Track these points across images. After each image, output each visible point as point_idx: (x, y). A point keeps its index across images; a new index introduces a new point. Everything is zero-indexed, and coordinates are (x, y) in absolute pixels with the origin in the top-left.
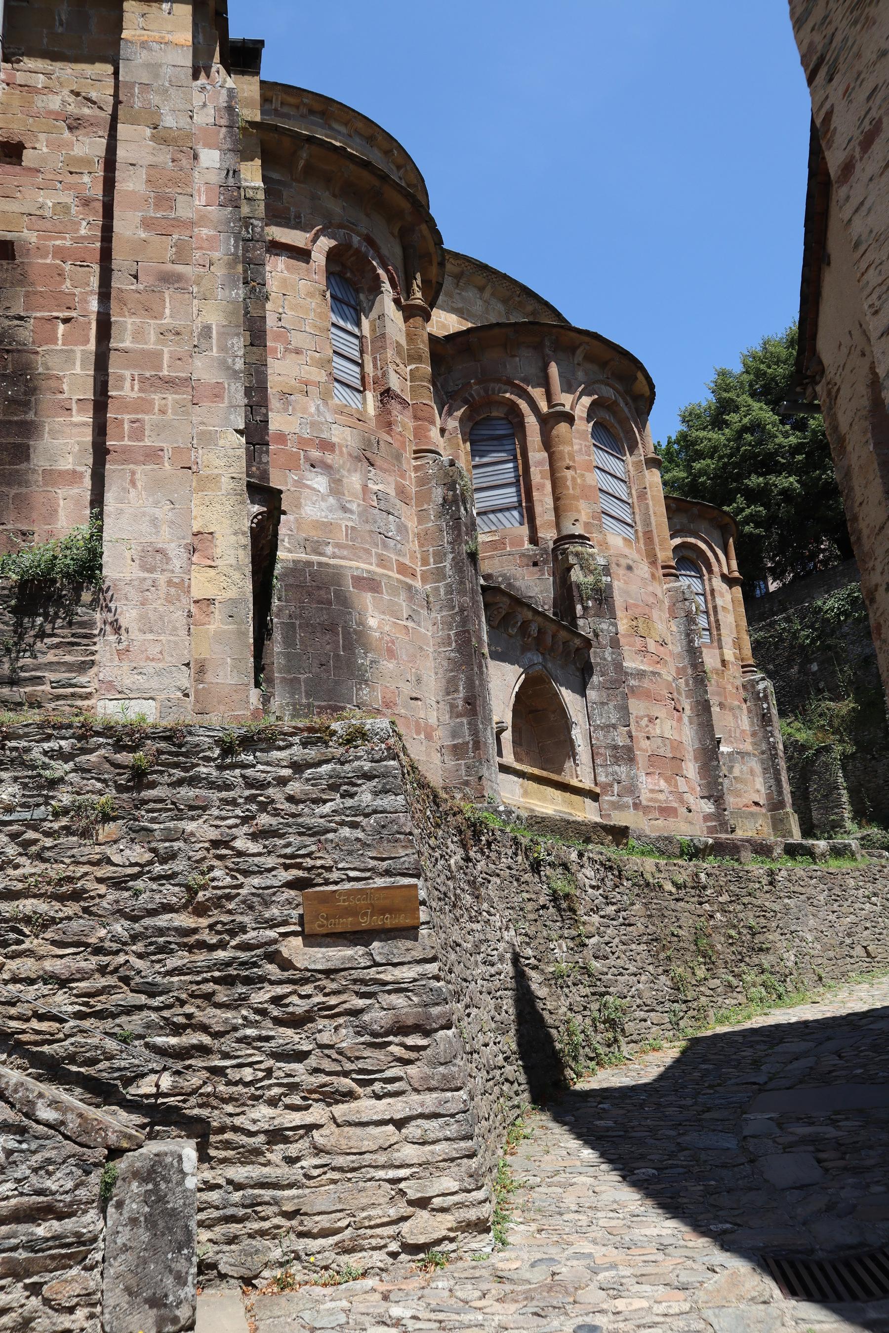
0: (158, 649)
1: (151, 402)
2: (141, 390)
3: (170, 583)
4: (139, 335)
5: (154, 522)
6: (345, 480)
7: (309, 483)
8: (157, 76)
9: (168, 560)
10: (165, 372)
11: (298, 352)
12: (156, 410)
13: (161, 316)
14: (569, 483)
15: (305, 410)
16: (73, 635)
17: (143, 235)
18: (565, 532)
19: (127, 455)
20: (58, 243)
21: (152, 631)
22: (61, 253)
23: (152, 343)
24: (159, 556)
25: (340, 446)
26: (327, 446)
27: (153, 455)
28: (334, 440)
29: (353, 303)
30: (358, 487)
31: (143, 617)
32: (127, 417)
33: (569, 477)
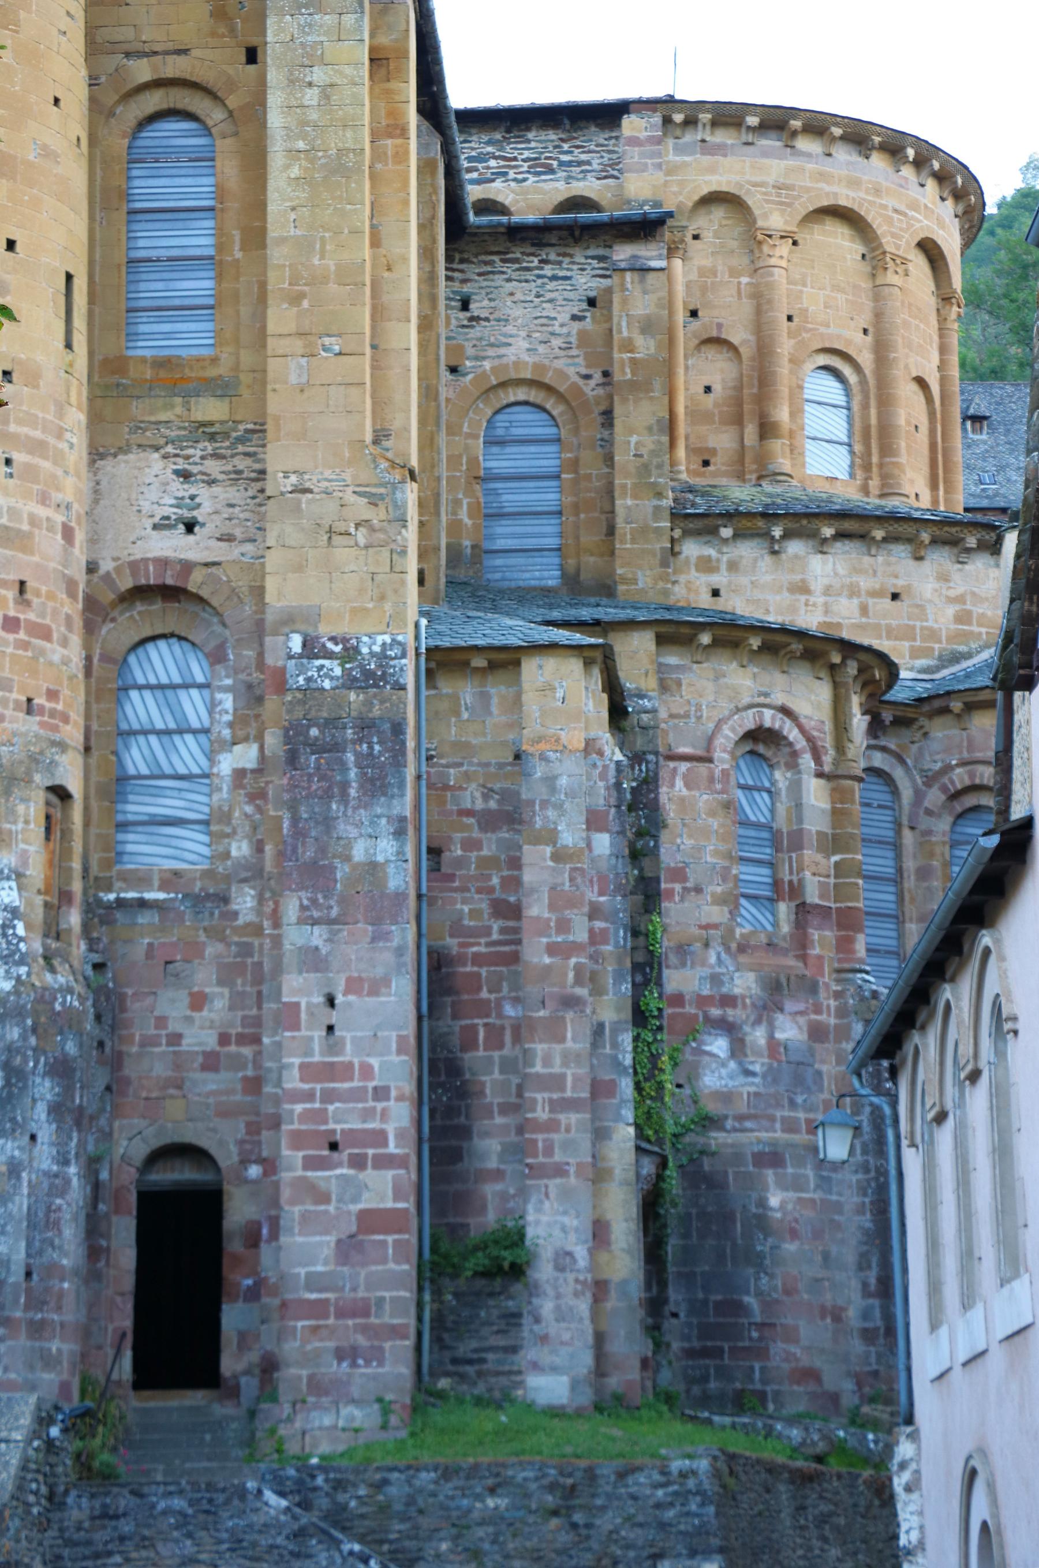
2: (551, 1111)
3: (577, 1281)
4: (547, 1061)
5: (564, 1229)
6: (748, 1039)
7: (707, 1048)
8: (553, 790)
10: (569, 1094)
11: (698, 890)
13: (562, 1040)
15: (704, 963)
17: (547, 960)
20: (475, 949)
22: (478, 959)
23: (557, 1069)
24: (568, 1259)
25: (743, 997)
26: (728, 1001)
28: (737, 991)
29: (767, 784)
30: (762, 1042)
31: (558, 1308)
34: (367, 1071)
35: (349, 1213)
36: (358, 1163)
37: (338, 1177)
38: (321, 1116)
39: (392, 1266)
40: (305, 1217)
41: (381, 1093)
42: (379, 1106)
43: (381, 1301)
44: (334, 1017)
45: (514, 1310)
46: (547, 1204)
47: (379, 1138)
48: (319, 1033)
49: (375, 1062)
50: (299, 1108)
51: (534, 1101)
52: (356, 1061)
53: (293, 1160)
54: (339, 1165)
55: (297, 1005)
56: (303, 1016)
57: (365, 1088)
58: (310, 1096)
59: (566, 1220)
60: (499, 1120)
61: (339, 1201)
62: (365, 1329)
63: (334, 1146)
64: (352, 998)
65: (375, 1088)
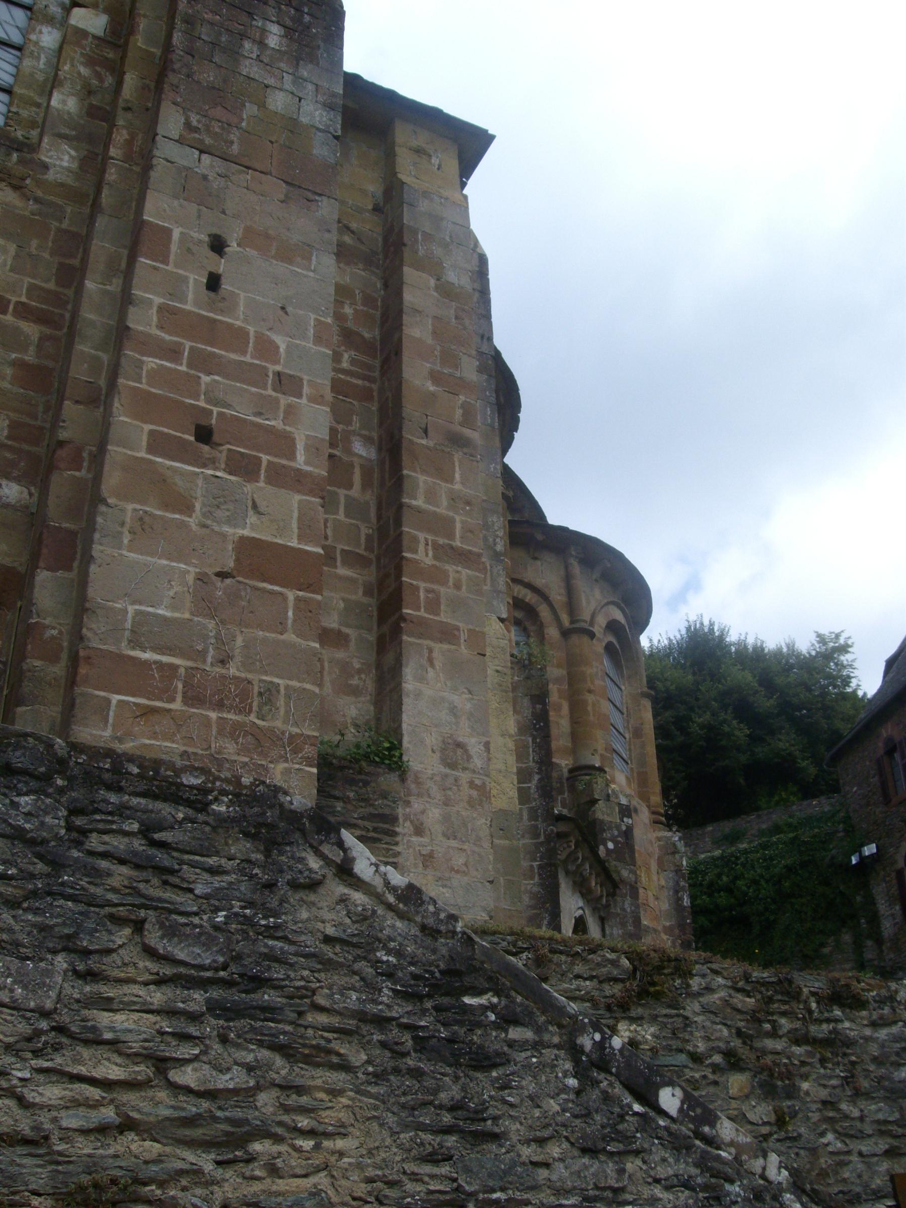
0: (462, 861)
1: (446, 573)
2: (435, 557)
4: (431, 496)
5: (453, 710)
9: (469, 757)
10: (458, 543)
12: (451, 583)
13: (450, 480)
14: (589, 708)
16: (375, 830)
18: (583, 762)
19: (424, 629)
21: (455, 838)
23: (442, 509)
24: (459, 752)
27: (448, 634)
31: (446, 818)
32: (422, 585)
33: (590, 701)
34: (267, 349)
35: (224, 536)
36: (245, 468)
37: (206, 478)
38: (190, 385)
39: (290, 637)
40: (143, 523)
41: (286, 383)
42: (284, 401)
43: (269, 694)
44: (222, 266)
45: (387, 811)
46: (431, 673)
47: (283, 444)
48: (195, 280)
49: (282, 343)
50: (151, 362)
51: (415, 540)
52: (252, 330)
53: (132, 437)
54: (211, 462)
55: (168, 232)
56: (174, 248)
57: (264, 372)
58: (174, 353)
59: (455, 698)
60: (342, 571)
61: (207, 514)
62: (234, 731)
63: (204, 434)
64: (251, 252)
65: (279, 374)
